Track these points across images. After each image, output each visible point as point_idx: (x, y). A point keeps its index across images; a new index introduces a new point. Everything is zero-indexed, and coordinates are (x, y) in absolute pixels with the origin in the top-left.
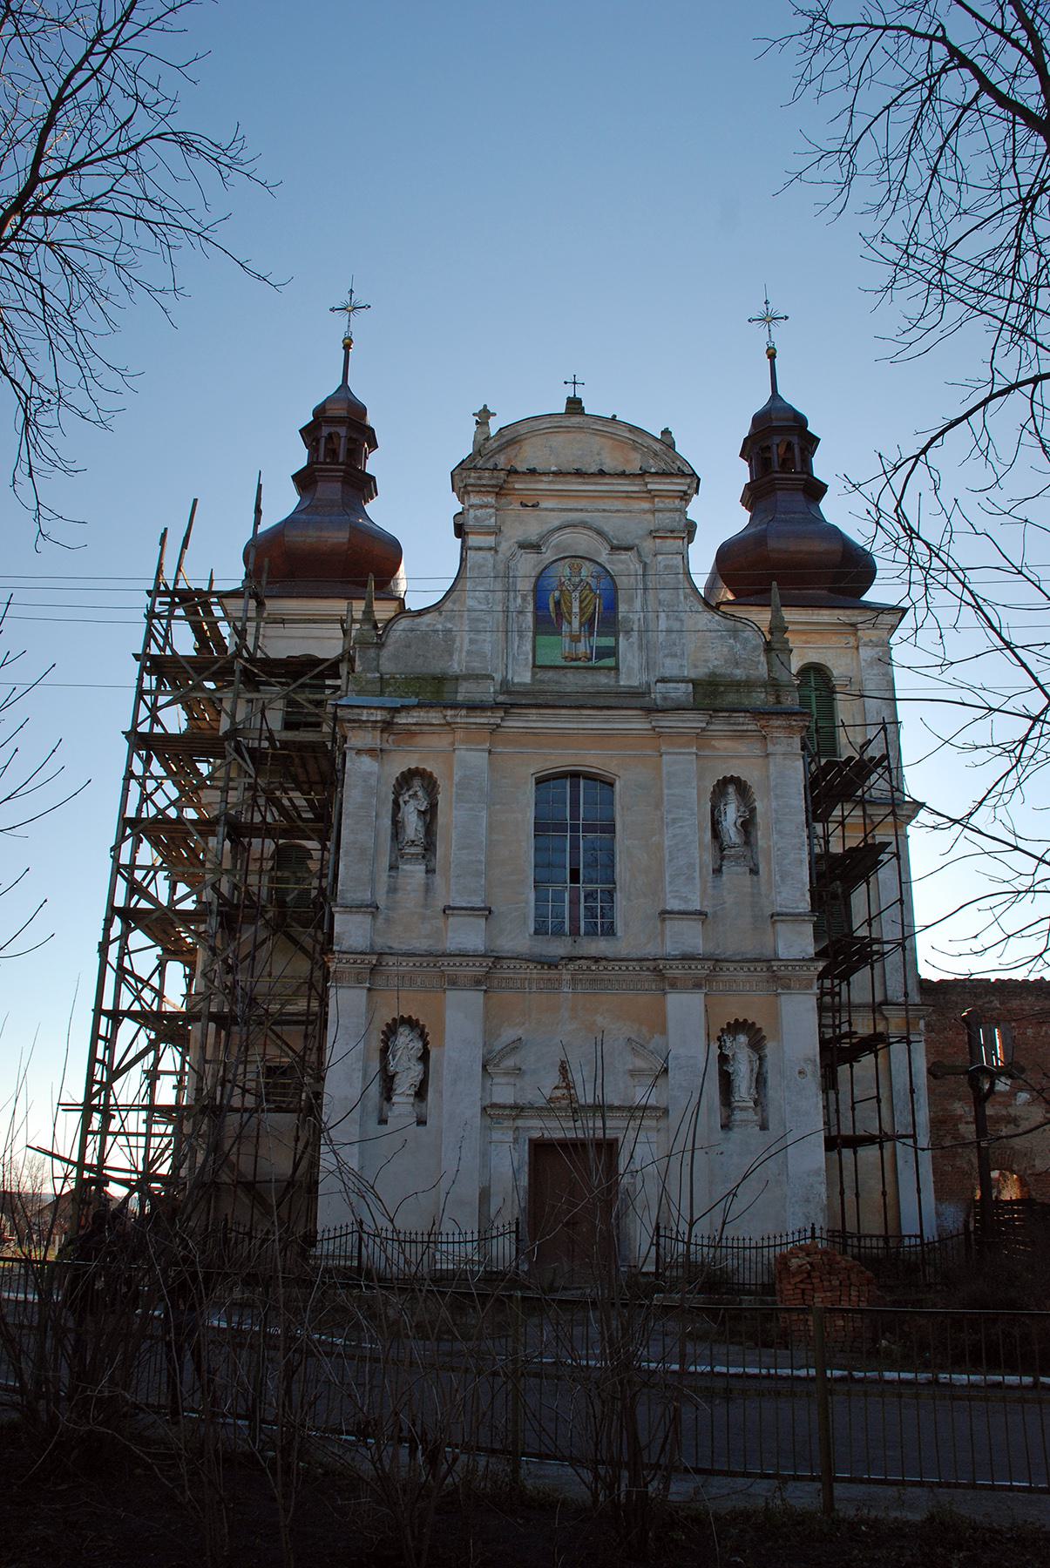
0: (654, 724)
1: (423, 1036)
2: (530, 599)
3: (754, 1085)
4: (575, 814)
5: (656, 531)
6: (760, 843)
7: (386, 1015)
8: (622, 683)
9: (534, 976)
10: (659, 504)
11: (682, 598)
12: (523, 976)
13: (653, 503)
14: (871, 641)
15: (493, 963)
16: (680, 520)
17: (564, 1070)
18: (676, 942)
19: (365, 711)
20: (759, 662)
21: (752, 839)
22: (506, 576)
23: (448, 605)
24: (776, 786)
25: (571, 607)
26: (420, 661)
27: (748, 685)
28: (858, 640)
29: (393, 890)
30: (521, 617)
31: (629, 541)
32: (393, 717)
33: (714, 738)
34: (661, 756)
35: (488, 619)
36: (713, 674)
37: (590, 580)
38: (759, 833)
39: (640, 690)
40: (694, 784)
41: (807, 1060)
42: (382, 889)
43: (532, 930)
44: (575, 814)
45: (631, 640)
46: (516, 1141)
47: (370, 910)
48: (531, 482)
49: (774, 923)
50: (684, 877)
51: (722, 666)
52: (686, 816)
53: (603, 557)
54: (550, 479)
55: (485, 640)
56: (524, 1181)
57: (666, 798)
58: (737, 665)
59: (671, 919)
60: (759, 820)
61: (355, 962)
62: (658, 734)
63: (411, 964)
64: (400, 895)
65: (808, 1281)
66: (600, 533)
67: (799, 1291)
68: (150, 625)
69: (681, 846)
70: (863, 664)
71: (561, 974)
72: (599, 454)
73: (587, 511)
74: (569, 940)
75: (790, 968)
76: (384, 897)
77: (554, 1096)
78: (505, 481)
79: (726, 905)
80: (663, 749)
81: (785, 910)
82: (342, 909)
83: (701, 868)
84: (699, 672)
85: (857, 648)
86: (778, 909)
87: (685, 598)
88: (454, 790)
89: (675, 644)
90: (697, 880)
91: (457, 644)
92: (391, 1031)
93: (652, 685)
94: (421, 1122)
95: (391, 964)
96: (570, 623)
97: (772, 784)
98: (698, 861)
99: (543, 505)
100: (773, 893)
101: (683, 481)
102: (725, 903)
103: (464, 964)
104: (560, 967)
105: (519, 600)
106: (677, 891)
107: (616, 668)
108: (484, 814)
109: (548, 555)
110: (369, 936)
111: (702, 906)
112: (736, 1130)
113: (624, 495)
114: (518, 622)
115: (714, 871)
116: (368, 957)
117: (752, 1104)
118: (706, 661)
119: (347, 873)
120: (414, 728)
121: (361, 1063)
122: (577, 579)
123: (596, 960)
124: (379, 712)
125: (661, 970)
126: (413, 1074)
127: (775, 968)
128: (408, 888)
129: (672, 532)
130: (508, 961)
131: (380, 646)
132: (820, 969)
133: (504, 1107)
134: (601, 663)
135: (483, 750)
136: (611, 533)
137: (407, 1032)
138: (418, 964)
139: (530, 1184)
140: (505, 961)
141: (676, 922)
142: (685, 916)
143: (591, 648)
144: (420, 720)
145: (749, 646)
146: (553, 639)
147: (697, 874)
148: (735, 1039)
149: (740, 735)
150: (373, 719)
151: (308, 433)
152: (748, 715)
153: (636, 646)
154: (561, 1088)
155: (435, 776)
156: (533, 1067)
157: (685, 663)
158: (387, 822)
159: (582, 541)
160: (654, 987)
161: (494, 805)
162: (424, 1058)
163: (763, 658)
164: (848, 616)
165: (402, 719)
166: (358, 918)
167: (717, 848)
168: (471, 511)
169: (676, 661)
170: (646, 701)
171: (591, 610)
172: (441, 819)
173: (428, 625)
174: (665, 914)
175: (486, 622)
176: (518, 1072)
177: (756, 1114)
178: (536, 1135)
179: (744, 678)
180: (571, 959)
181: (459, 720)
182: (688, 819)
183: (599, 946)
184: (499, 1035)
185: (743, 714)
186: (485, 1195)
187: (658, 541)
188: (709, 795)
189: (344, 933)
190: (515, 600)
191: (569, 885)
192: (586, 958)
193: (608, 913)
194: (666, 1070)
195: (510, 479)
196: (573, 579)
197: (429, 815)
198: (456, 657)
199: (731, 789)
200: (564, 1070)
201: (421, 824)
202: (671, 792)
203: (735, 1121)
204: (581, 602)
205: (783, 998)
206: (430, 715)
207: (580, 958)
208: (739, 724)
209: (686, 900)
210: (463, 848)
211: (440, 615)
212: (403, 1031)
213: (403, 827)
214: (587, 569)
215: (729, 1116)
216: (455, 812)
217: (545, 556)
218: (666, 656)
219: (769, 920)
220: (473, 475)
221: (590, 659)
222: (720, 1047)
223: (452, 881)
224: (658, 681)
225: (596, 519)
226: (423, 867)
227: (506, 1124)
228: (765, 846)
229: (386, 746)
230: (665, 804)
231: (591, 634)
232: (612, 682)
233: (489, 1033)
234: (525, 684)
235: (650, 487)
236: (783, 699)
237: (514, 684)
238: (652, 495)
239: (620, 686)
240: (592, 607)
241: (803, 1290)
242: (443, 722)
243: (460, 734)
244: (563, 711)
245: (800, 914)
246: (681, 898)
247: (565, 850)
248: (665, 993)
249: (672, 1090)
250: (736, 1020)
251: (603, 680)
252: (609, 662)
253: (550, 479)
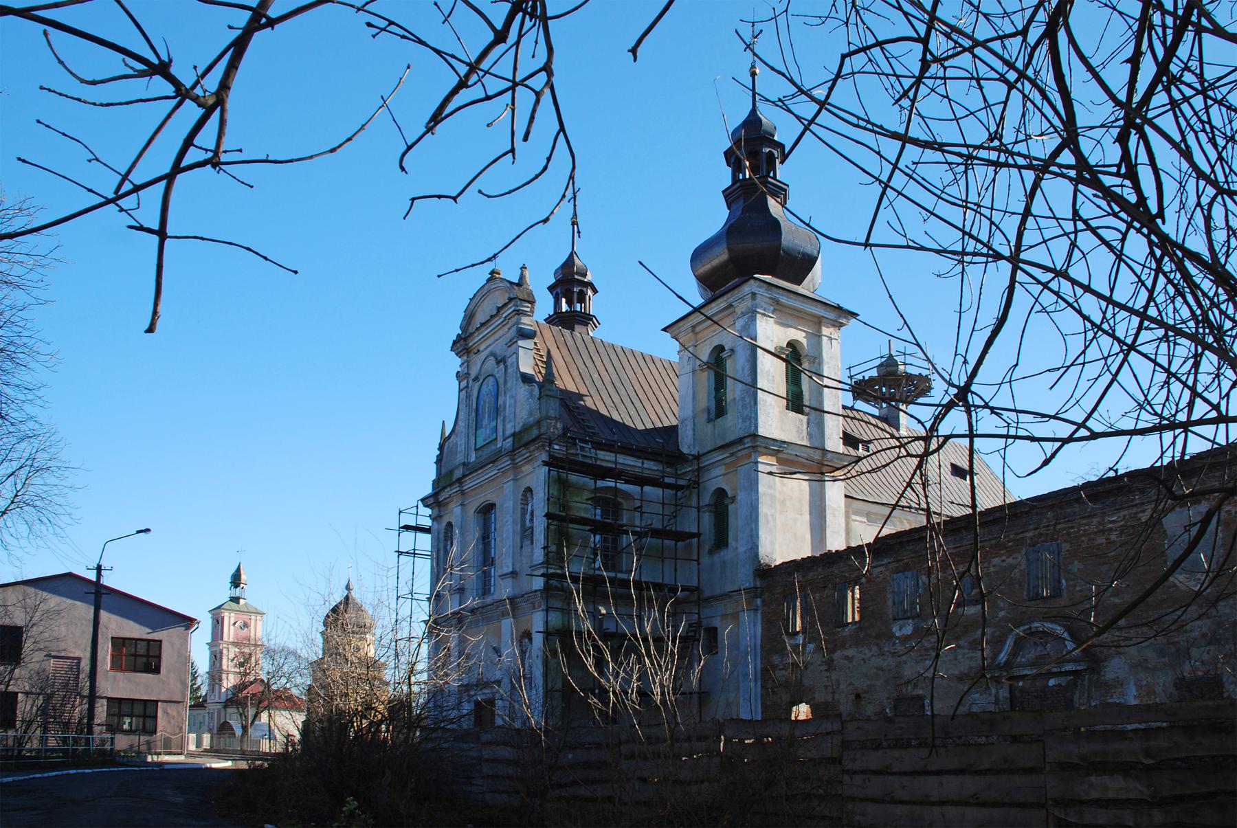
99: (481, 348)
164: (726, 301)
235: (504, 316)
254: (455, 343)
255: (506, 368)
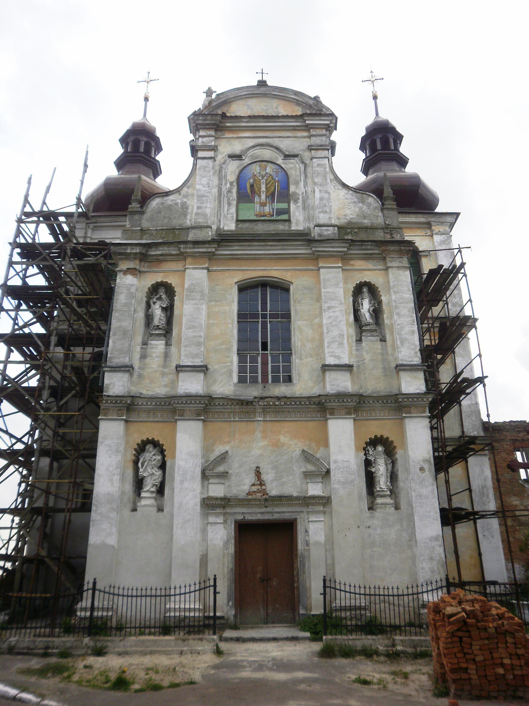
0: (313, 249)
1: (162, 452)
2: (235, 184)
3: (389, 480)
4: (264, 308)
5: (312, 146)
6: (386, 321)
7: (138, 438)
8: (293, 228)
9: (237, 410)
10: (313, 132)
11: (329, 181)
12: (229, 410)
13: (310, 132)
14: (440, 232)
15: (209, 401)
16: (326, 140)
17: (258, 473)
18: (333, 385)
19: (129, 247)
20: (378, 216)
21: (380, 322)
22: (220, 173)
23: (185, 189)
24: (394, 286)
25: (260, 188)
26: (166, 221)
27: (372, 228)
28: (432, 231)
29: (143, 356)
30: (229, 194)
31: (296, 152)
32: (147, 251)
33: (352, 259)
34: (319, 270)
35: (208, 195)
36: (350, 223)
37: (272, 173)
38: (385, 316)
39: (304, 232)
40: (341, 285)
41: (426, 461)
42: (137, 356)
43: (235, 379)
44: (264, 308)
45: (298, 204)
46: (225, 522)
47: (127, 369)
48: (236, 122)
49: (398, 372)
50: (336, 343)
51: (355, 218)
52: (336, 305)
53: (280, 161)
54: (247, 120)
55: (206, 207)
56: (232, 549)
57: (323, 294)
58: (365, 217)
59: (329, 370)
60: (384, 307)
61: (116, 403)
62: (315, 257)
63: (154, 404)
64: (148, 360)
65: (464, 629)
66: (277, 148)
67: (457, 639)
68: (19, 226)
69: (334, 324)
70: (436, 243)
71: (255, 409)
72: (277, 108)
73: (270, 137)
74: (260, 386)
75: (410, 400)
76: (138, 362)
77: (251, 490)
78: (220, 122)
79: (366, 361)
80: (321, 265)
81: (404, 363)
82: (109, 369)
83: (348, 338)
84: (343, 221)
85: (432, 236)
86: (400, 362)
87: (331, 181)
88: (185, 293)
89: (325, 206)
90: (346, 345)
91: (190, 210)
92: (141, 448)
93: (312, 229)
94: (160, 509)
95: (140, 404)
96: (260, 196)
97: (391, 284)
98: (345, 333)
100: (396, 353)
101: (327, 118)
102: (364, 360)
103: (189, 402)
104: (254, 404)
105: (228, 185)
106: (333, 352)
107: (289, 221)
108: (204, 307)
109: (247, 161)
110: (126, 385)
111: (349, 360)
112: (378, 510)
113: (292, 128)
114: (227, 197)
115: (356, 341)
116: (125, 399)
117: (389, 493)
118: (345, 215)
119: (114, 346)
120: (160, 258)
121: (119, 470)
122: (264, 173)
123: (278, 398)
124: (138, 248)
125: (323, 403)
126: (154, 478)
127: (400, 400)
128: (154, 355)
129: (321, 146)
130: (218, 400)
131: (142, 213)
132: (430, 399)
133: (217, 499)
134: (279, 218)
135: (203, 268)
136: (285, 149)
137: (151, 449)
138: (158, 404)
139: (236, 552)
140: (216, 400)
141: (332, 372)
142: (338, 368)
143: (273, 209)
144: (164, 252)
145: (372, 207)
146: (249, 205)
147: (345, 341)
148: (375, 449)
149: (367, 257)
150: (134, 251)
151: (124, 141)
152: (373, 243)
153: (301, 208)
154: (257, 485)
155: (173, 285)
156: (237, 471)
157: (332, 216)
158: (141, 314)
159: (267, 154)
160: (319, 416)
161: (210, 301)
162: (163, 466)
163: (380, 214)
164: (425, 218)
165: (153, 252)
166: (120, 375)
167: (358, 327)
168: (200, 139)
169: (327, 216)
170: (309, 237)
171: (272, 189)
172: (176, 312)
173: (172, 200)
174: (326, 368)
175: (207, 197)
176: (224, 475)
177: (391, 499)
178: (240, 517)
179: (369, 225)
180: (261, 398)
181: (188, 250)
182: (337, 307)
183: (281, 390)
184: (214, 450)
185: (370, 243)
186: (204, 560)
187: (313, 152)
188: (351, 293)
189: (110, 384)
190: (226, 184)
191: (261, 352)
192: (272, 397)
193: (288, 369)
194: (328, 472)
195: (223, 121)
196: (261, 173)
197: (169, 310)
198: (188, 217)
199: (365, 290)
200: (258, 473)
201: (163, 315)
202: (326, 290)
203: (378, 504)
204: (266, 185)
205: (407, 421)
206: (170, 249)
207: (268, 397)
208: (368, 250)
209: (338, 357)
210: (190, 328)
211: (180, 194)
212: (149, 447)
213: (152, 319)
214: (270, 169)
215: (372, 502)
216: (185, 306)
217: (244, 161)
218: (320, 212)
219: (394, 370)
220: (201, 118)
221: (273, 216)
222: (365, 454)
223: (183, 349)
224: (315, 226)
225: (276, 142)
226: (164, 342)
227: (218, 511)
228: (389, 323)
229: (143, 269)
230: (323, 297)
231: (273, 201)
232: (287, 228)
233: (207, 449)
234: (231, 231)
235: (307, 122)
236: (394, 236)
237: (224, 231)
238: (308, 128)
239: (292, 230)
240: (273, 187)
241: (461, 638)
242: (178, 252)
243: (189, 260)
244: (255, 244)
245: (415, 365)
246: (335, 357)
247: (258, 332)
248: (326, 420)
249: (334, 484)
250: (376, 436)
251: (281, 227)
252: (285, 217)
253: (247, 120)
254: (195, 114)
255: (306, 166)
